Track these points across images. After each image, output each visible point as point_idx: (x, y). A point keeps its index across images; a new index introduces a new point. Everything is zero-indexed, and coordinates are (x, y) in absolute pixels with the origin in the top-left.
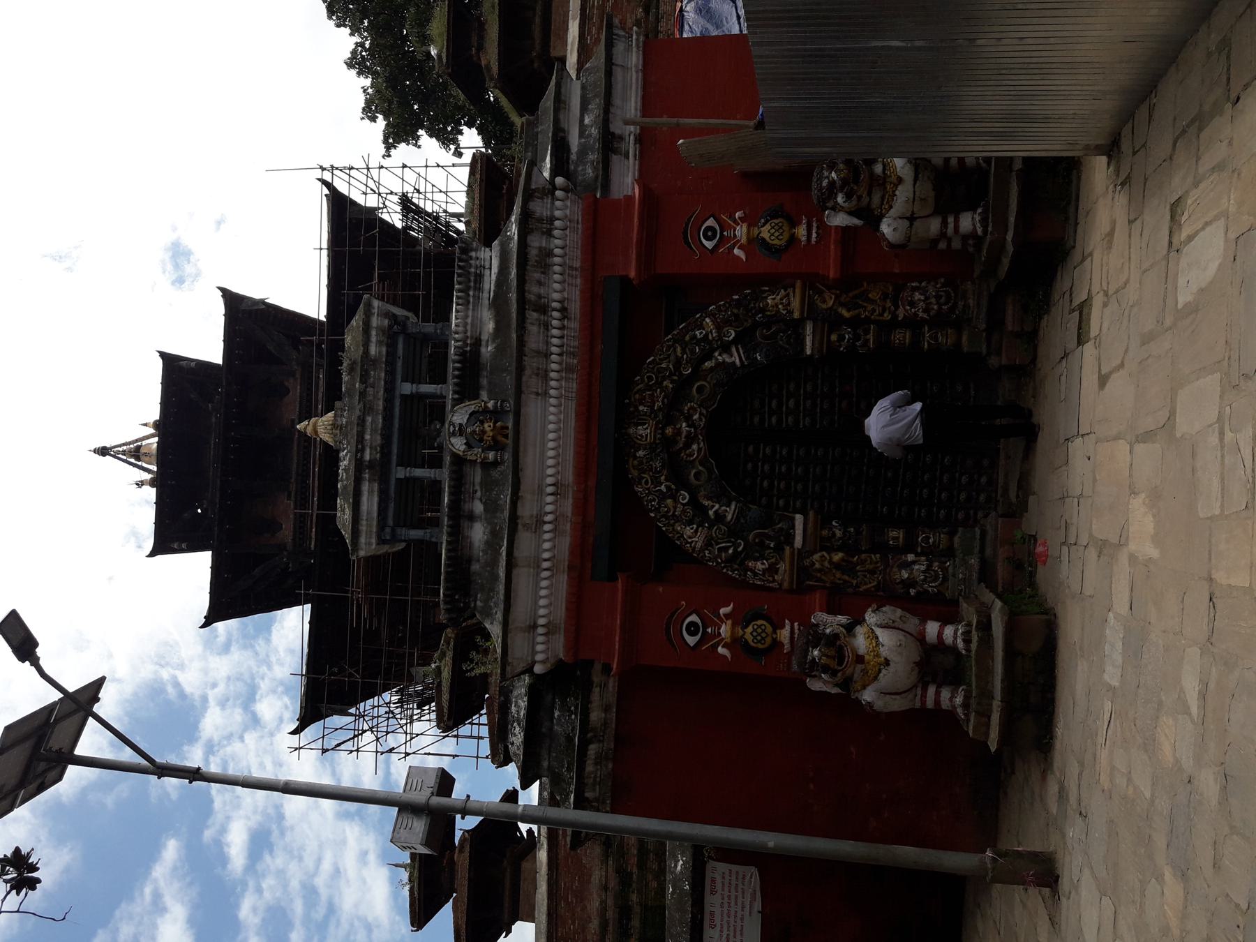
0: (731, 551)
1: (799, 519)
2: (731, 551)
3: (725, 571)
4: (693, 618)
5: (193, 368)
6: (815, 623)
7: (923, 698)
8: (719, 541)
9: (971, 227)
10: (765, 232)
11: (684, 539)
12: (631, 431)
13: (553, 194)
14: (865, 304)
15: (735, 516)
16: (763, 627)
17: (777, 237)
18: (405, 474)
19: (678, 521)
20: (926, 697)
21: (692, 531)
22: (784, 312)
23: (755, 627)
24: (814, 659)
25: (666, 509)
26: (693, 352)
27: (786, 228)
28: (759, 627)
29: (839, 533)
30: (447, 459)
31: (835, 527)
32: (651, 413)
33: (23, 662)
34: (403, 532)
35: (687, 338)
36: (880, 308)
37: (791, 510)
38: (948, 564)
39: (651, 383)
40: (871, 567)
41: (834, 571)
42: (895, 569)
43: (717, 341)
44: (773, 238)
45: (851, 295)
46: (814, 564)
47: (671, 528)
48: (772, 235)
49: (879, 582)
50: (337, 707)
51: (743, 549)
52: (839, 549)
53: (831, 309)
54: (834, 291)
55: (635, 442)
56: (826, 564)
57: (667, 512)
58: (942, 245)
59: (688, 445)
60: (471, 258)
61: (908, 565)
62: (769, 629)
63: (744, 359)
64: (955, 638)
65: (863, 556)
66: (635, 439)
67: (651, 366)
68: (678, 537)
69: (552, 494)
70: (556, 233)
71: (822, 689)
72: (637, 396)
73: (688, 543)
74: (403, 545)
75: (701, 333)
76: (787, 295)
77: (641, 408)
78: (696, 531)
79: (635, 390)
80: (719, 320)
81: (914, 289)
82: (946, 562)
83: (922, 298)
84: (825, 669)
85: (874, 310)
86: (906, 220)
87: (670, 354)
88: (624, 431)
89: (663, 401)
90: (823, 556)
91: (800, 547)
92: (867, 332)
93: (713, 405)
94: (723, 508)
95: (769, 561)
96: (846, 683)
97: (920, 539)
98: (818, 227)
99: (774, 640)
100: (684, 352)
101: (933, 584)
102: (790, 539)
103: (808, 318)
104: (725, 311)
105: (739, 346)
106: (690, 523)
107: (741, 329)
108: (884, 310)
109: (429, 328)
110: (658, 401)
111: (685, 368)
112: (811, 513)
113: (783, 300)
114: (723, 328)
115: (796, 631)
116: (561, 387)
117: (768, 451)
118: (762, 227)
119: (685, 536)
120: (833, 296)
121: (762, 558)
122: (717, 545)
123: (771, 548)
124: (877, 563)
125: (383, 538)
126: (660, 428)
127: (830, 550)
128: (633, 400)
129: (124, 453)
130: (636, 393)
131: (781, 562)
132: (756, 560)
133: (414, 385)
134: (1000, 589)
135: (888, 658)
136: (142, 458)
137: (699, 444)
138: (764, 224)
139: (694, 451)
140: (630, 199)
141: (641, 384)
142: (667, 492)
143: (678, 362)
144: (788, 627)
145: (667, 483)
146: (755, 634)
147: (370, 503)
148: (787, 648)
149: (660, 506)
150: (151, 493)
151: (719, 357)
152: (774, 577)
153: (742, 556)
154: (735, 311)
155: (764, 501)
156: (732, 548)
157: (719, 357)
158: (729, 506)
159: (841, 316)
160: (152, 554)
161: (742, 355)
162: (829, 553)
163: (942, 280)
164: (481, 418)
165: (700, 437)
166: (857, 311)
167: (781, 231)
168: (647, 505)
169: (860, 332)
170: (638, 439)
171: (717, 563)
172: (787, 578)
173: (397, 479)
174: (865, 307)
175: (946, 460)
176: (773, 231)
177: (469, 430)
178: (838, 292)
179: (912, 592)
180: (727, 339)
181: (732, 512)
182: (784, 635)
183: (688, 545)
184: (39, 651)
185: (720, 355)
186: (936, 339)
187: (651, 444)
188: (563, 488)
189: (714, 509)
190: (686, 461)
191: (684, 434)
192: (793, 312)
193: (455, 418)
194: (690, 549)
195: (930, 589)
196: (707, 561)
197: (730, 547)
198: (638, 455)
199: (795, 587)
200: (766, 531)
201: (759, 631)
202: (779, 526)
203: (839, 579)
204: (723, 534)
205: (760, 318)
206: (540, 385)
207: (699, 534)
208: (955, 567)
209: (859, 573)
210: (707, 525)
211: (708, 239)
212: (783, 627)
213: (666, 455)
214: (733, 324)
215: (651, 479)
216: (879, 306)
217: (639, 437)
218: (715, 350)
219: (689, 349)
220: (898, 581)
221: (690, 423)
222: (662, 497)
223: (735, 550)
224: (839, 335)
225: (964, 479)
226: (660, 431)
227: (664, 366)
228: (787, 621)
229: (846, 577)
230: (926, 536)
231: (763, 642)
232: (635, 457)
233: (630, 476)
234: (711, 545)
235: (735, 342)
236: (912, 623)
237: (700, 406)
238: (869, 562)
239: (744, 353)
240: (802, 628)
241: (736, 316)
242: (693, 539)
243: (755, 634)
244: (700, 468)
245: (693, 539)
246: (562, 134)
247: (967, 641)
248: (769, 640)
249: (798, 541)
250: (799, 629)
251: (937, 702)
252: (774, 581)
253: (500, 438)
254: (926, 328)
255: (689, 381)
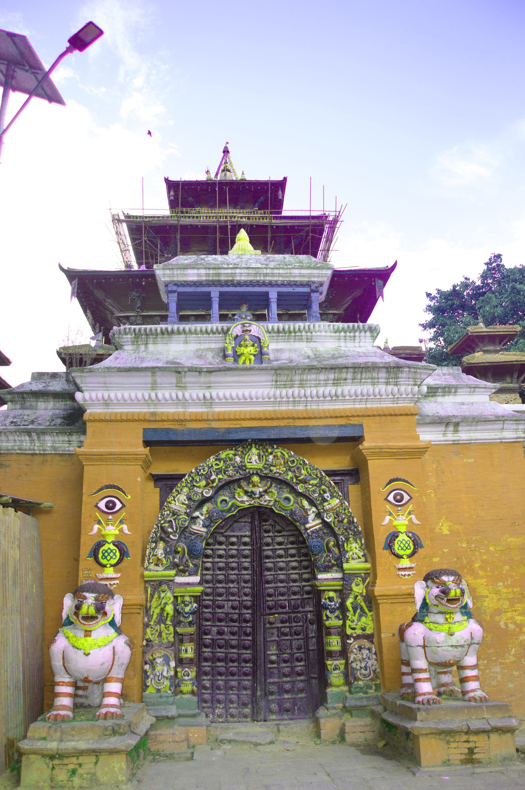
0: (170, 530)
1: (196, 579)
2: (170, 530)
3: (155, 526)
4: (119, 505)
5: (278, 197)
6: (115, 597)
7: (61, 684)
8: (177, 521)
9: (421, 692)
10: (402, 537)
11: (177, 495)
12: (254, 450)
13: (415, 385)
14: (357, 614)
15: (196, 531)
16: (114, 557)
17: (400, 546)
18: (215, 297)
19: (190, 489)
20: (62, 685)
21: (183, 500)
22: (347, 556)
23: (114, 551)
24: (85, 598)
25: (198, 480)
26: (314, 492)
27: (409, 552)
28: (115, 554)
29: (187, 609)
30: (225, 325)
31: (192, 606)
32: (268, 465)
33: (70, 41)
34: (174, 297)
35: (323, 487)
36: (354, 626)
37: (205, 572)
38: (169, 692)
39: (289, 463)
40: (164, 635)
41: (159, 608)
42: (163, 652)
43: (323, 509)
44: (399, 543)
45: (363, 604)
46: (163, 592)
47: (184, 485)
48: (401, 542)
49: (151, 641)
50: (76, 290)
51: (172, 539)
52: (176, 610)
53: (351, 590)
54: (365, 591)
55: (246, 454)
56: (163, 602)
57: (196, 481)
58: (405, 669)
59: (246, 492)
60: (365, 332)
61: (167, 662)
62: (113, 562)
63: (311, 529)
64: (107, 706)
65: (171, 629)
66: (248, 454)
67: (301, 462)
68: (178, 491)
69: (204, 396)
70: (390, 388)
71: (64, 605)
72: (279, 454)
73: (174, 497)
74: (166, 301)
75: (328, 497)
76: (359, 558)
77: (271, 457)
78: (183, 504)
79: (284, 452)
80: (338, 509)
81: (369, 649)
82: (170, 690)
83: (365, 657)
84: (78, 607)
85: (353, 621)
86: (423, 641)
87: (310, 475)
88: (253, 445)
89: (278, 473)
90: (170, 599)
91: (175, 581)
92: (337, 617)
93: (278, 510)
94: (201, 522)
95: (164, 559)
96: (69, 623)
97: (186, 669)
98: (409, 575)
99: (105, 566)
100: (312, 485)
101: (153, 682)
102: (182, 572)
103: (344, 574)
104: (345, 513)
105: (321, 525)
106: (189, 499)
107: (333, 525)
108: (354, 629)
109: (315, 307)
110: (277, 469)
111: (302, 487)
112: (200, 589)
113: (356, 554)
114: (333, 513)
115: (112, 582)
116: (282, 398)
117: (247, 552)
118: (406, 534)
119: (179, 496)
120: (361, 591)
121: (166, 553)
122: (174, 519)
123: (174, 558)
124: (167, 638)
125: (169, 285)
126: (257, 472)
127: (175, 603)
128: (276, 451)
129: (226, 163)
130: (281, 453)
131: (163, 568)
132: (165, 550)
133: (276, 300)
134: (152, 733)
135: (89, 656)
136: (224, 173)
137: (247, 501)
138: (408, 536)
139: (242, 497)
140: (417, 438)
141: (289, 456)
142: (211, 481)
143: (304, 481)
144: (115, 576)
145: (217, 480)
146: (109, 551)
147: (192, 275)
148: (101, 576)
149: (200, 475)
150: (203, 177)
151: (311, 511)
152: (152, 563)
153: (167, 539)
154: (345, 521)
155: (209, 552)
156: (172, 531)
157: (311, 511)
158: (203, 526)
159: (348, 597)
160: (167, 180)
161: (314, 528)
162: (173, 602)
163: (378, 670)
164: (256, 345)
165: (253, 501)
166: (351, 609)
167: (405, 548)
168: (200, 466)
169: (337, 613)
170: (249, 456)
171: (160, 521)
172: (151, 573)
173: (210, 293)
174: (354, 615)
175: (246, 682)
176: (404, 542)
177: (247, 337)
178: (364, 594)
179: (147, 667)
180: (325, 516)
181: (199, 529)
182: (109, 572)
183: (172, 498)
184: (77, 52)
185: (313, 512)
186: (336, 669)
187: (245, 466)
188: (209, 404)
189: (201, 515)
190: (234, 493)
191: (254, 489)
192: (347, 562)
193: (255, 327)
194: (170, 500)
195: (150, 680)
196: (162, 513)
197: (173, 529)
198: (237, 457)
199: (146, 579)
200: (186, 555)
201: (112, 554)
202: (191, 565)
203: (153, 612)
204: (182, 524)
205: (342, 539)
206: (283, 383)
207: (181, 505)
208: (167, 697)
209: (158, 626)
210: (188, 511)
211: (395, 497)
212: (115, 572)
213: (238, 478)
214: (336, 520)
215: (219, 469)
216: (357, 625)
217: (249, 457)
218: (317, 508)
219: (315, 489)
220: (154, 655)
221: (263, 494)
222: (207, 477)
223: (171, 533)
224: (333, 597)
225: (234, 697)
226: (255, 472)
227: (303, 472)
228: (119, 575)
229: (155, 616)
230: (189, 674)
231: (104, 557)
232: (235, 455)
233: (221, 452)
234: (174, 514)
235: (324, 522)
236: (118, 672)
237: (276, 501)
238: (167, 632)
239: (316, 529)
240: (115, 586)
241: (342, 521)
242: (177, 502)
243: (109, 551)
244: (230, 504)
245: (177, 502)
246: (453, 390)
247: (105, 716)
248: (104, 562)
249: (179, 579)
250: (114, 584)
251: (58, 695)
252: (149, 563)
253: (243, 358)
254: (343, 662)
255: (293, 490)
